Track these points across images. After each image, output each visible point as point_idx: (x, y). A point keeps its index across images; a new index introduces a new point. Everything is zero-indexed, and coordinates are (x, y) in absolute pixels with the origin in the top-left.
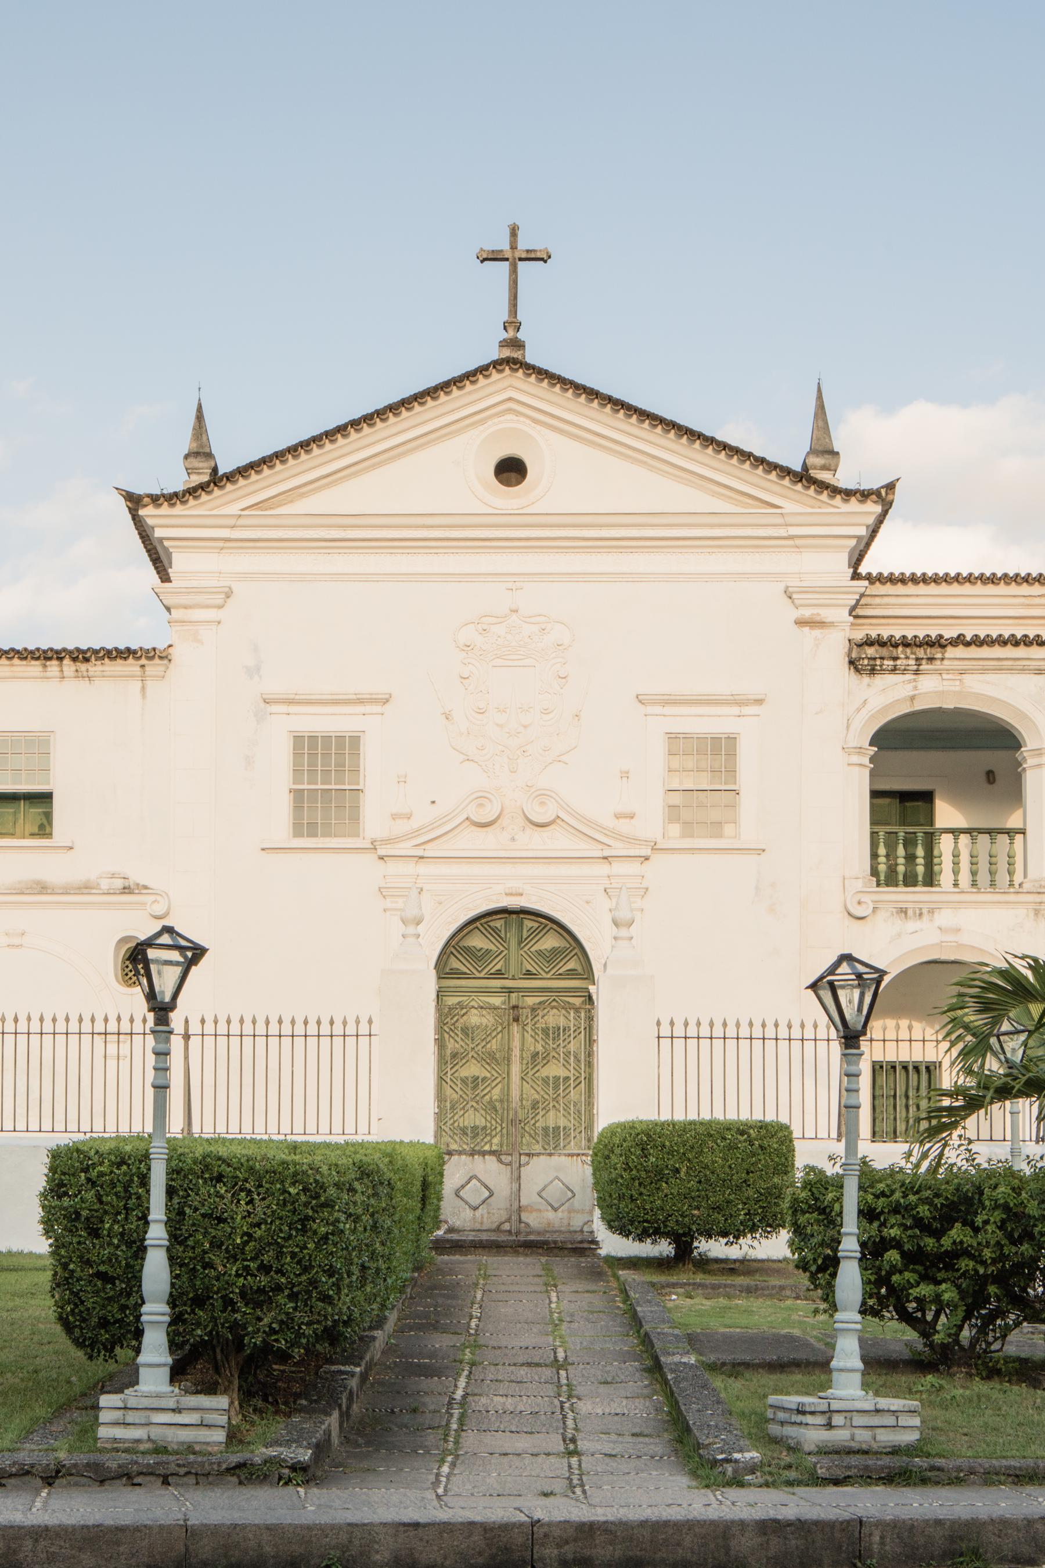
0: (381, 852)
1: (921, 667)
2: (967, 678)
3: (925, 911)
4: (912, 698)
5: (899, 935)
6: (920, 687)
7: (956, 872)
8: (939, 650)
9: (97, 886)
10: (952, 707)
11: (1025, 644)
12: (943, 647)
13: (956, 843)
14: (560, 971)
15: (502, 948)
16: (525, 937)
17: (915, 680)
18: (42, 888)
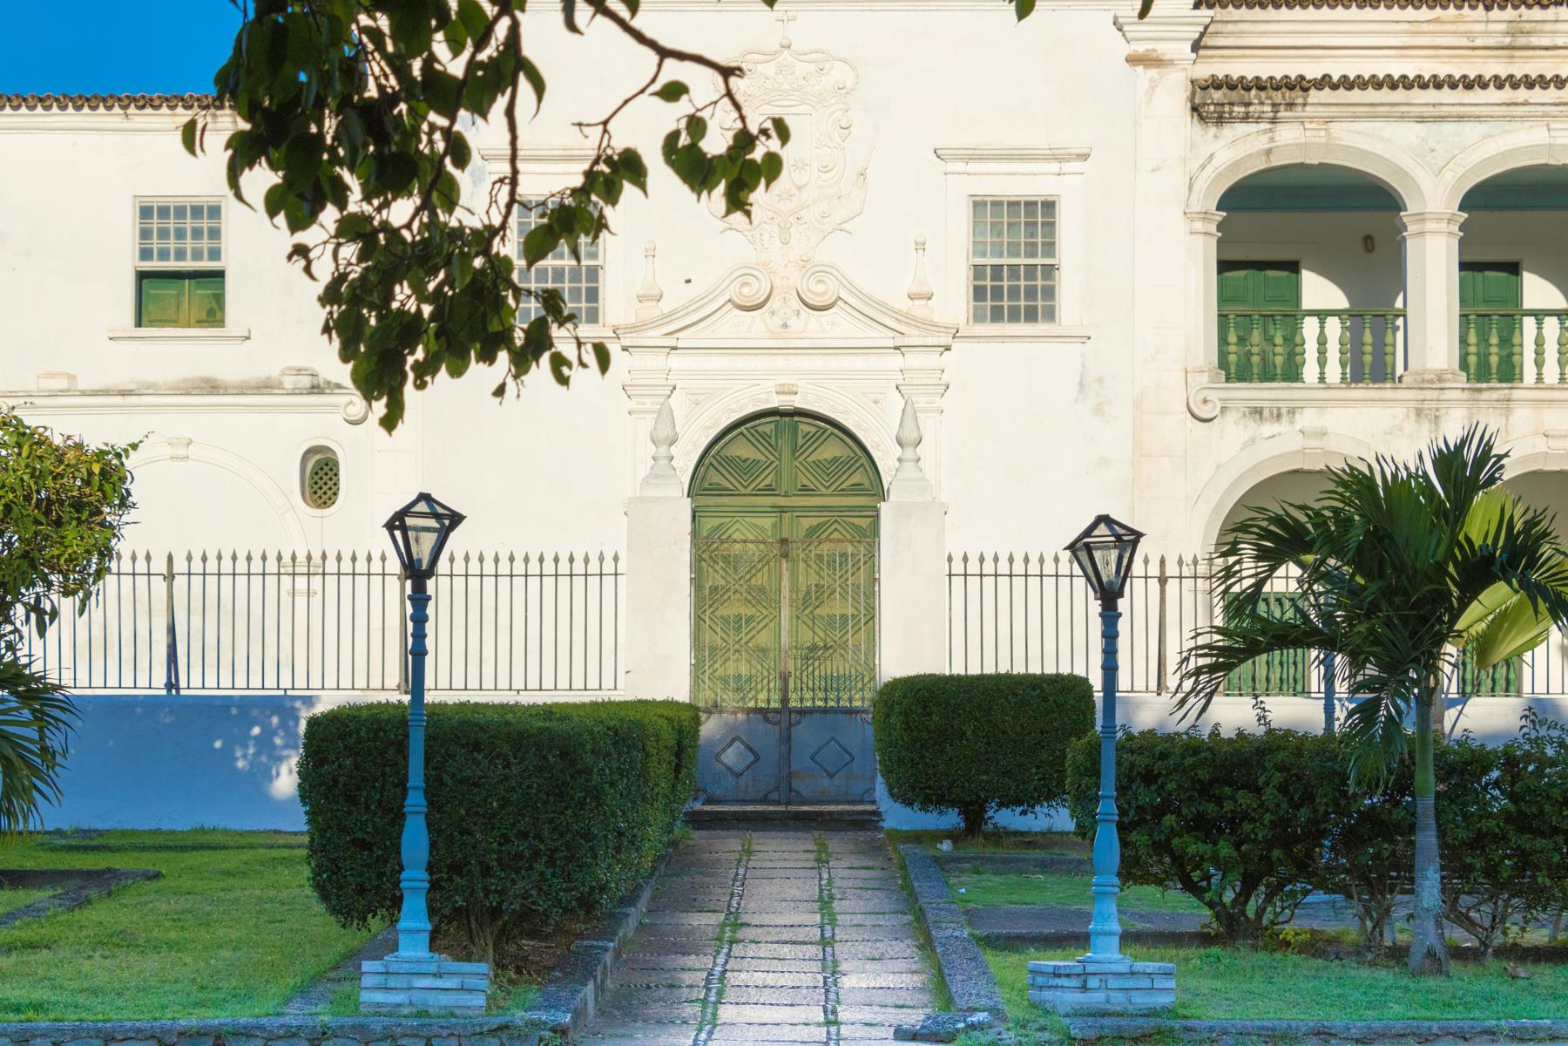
0: (626, 342)
1: (1279, 115)
2: (1336, 128)
3: (1284, 411)
4: (1269, 152)
5: (1253, 441)
6: (1277, 138)
7: (1322, 362)
8: (1301, 93)
9: (280, 386)
10: (1316, 162)
11: (1404, 87)
12: (1305, 90)
13: (1322, 328)
14: (843, 487)
15: (772, 459)
16: (800, 444)
17: (1271, 130)
18: (213, 387)
